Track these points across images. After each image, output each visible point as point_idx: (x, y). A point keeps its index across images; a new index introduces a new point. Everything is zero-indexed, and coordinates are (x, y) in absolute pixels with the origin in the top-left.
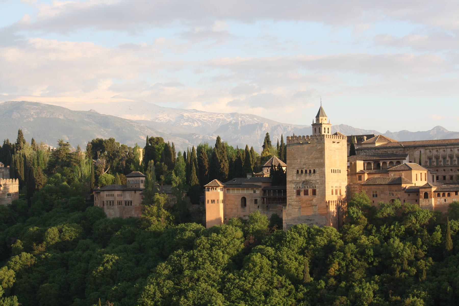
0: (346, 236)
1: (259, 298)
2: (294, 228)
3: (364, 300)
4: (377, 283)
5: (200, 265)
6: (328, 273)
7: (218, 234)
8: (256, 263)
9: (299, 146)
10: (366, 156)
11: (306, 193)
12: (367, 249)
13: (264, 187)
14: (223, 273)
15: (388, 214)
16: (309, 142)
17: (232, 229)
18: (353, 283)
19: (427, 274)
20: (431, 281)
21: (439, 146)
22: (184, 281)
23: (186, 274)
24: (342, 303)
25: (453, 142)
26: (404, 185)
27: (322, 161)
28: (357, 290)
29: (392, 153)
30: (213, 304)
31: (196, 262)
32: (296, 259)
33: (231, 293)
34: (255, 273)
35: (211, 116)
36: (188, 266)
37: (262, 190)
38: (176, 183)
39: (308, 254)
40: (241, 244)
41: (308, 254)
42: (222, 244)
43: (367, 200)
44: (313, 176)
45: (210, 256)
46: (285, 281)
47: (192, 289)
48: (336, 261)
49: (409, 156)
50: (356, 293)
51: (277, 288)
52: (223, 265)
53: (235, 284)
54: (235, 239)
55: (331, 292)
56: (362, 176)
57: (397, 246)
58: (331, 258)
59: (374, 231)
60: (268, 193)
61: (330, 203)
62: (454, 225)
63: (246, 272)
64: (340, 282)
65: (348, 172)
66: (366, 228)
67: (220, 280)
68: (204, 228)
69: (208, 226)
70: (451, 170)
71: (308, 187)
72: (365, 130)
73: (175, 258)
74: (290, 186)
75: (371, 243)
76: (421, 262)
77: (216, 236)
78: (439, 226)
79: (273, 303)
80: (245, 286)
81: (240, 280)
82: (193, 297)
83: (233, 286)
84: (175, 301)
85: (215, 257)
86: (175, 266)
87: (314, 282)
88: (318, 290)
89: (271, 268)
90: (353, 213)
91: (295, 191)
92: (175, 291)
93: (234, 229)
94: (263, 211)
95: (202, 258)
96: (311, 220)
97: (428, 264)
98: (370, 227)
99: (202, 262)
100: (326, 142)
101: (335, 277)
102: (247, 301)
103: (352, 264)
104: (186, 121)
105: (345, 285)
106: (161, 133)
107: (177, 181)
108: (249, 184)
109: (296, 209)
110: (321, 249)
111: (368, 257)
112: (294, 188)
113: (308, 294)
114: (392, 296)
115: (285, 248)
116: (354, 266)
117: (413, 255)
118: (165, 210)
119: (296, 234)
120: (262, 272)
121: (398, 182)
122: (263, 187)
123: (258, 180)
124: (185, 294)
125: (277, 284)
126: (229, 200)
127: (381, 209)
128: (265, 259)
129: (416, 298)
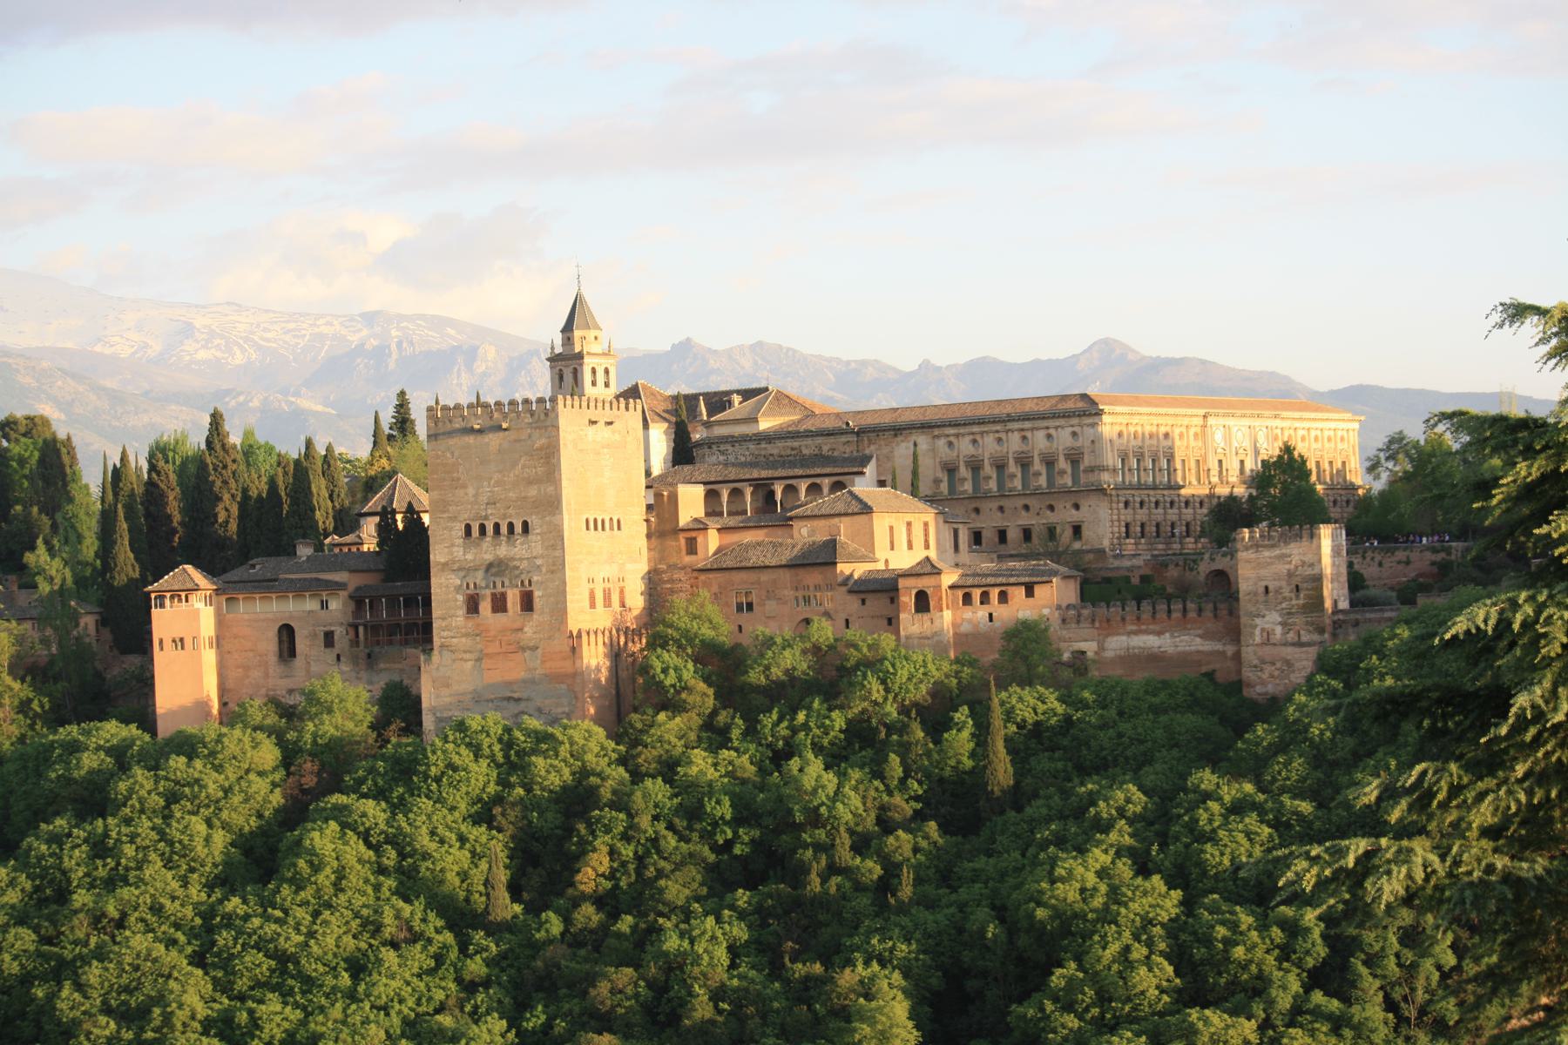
0: (639, 754)
1: (329, 981)
2: (456, 731)
3: (696, 979)
4: (742, 915)
5: (127, 869)
6: (572, 884)
7: (190, 759)
8: (321, 858)
9: (470, 439)
10: (726, 465)
11: (499, 605)
12: (710, 799)
13: (358, 589)
14: (209, 896)
15: (787, 672)
16: (505, 425)
17: (240, 740)
18: (661, 920)
19: (918, 881)
20: (931, 905)
21: (979, 423)
22: (72, 929)
23: (77, 905)
24: (621, 992)
25: (1028, 407)
26: (844, 568)
27: (550, 489)
28: (672, 943)
29: (816, 452)
30: (169, 1005)
31: (113, 858)
32: (462, 839)
33: (234, 966)
34: (318, 894)
35: (292, 326)
36: (87, 875)
37: (351, 597)
38: (51, 580)
39: (504, 822)
40: (272, 792)
41: (504, 822)
42: (203, 794)
43: (717, 625)
44: (522, 544)
45: (163, 836)
46: (424, 920)
47: (101, 955)
48: (602, 842)
49: (878, 459)
50: (666, 954)
51: (394, 945)
52: (207, 869)
53: (250, 936)
54: (252, 776)
55: (583, 952)
56: (700, 540)
57: (813, 783)
58: (583, 832)
59: (735, 733)
60: (371, 607)
61: (584, 637)
62: (1020, 706)
63: (286, 890)
64: (614, 916)
65: (649, 527)
66: (709, 725)
67: (198, 921)
68: (147, 737)
69: (165, 729)
70: (1026, 508)
71: (507, 583)
72: (845, 358)
73: (44, 847)
74: (443, 580)
75: (728, 774)
76: (897, 839)
77: (183, 767)
78: (965, 709)
79: (379, 997)
80: (282, 940)
81: (267, 918)
82: (102, 984)
83: (240, 941)
84: (41, 999)
85: (180, 842)
86: (42, 878)
87: (525, 920)
88: (536, 947)
89: (373, 874)
90: (665, 671)
91: (460, 598)
92: (41, 965)
93: (247, 739)
94: (354, 674)
95: (134, 847)
96: (518, 700)
97: (924, 844)
98: (723, 717)
99: (135, 859)
100: (562, 422)
101: (599, 901)
102: (291, 992)
103: (659, 852)
104: (203, 347)
105: (634, 928)
106: (114, 390)
107: (53, 573)
108: (305, 579)
109: (466, 661)
110: (549, 800)
111: (715, 824)
112: (458, 589)
113: (504, 964)
114: (793, 961)
115: (424, 800)
116: (665, 859)
117: (873, 815)
118: (15, 679)
119: (464, 751)
120: (342, 890)
121: (823, 556)
122: (351, 588)
123: (337, 564)
124: (76, 973)
125: (394, 929)
126: (236, 637)
127: (762, 655)
128: (352, 843)
129: (875, 966)
